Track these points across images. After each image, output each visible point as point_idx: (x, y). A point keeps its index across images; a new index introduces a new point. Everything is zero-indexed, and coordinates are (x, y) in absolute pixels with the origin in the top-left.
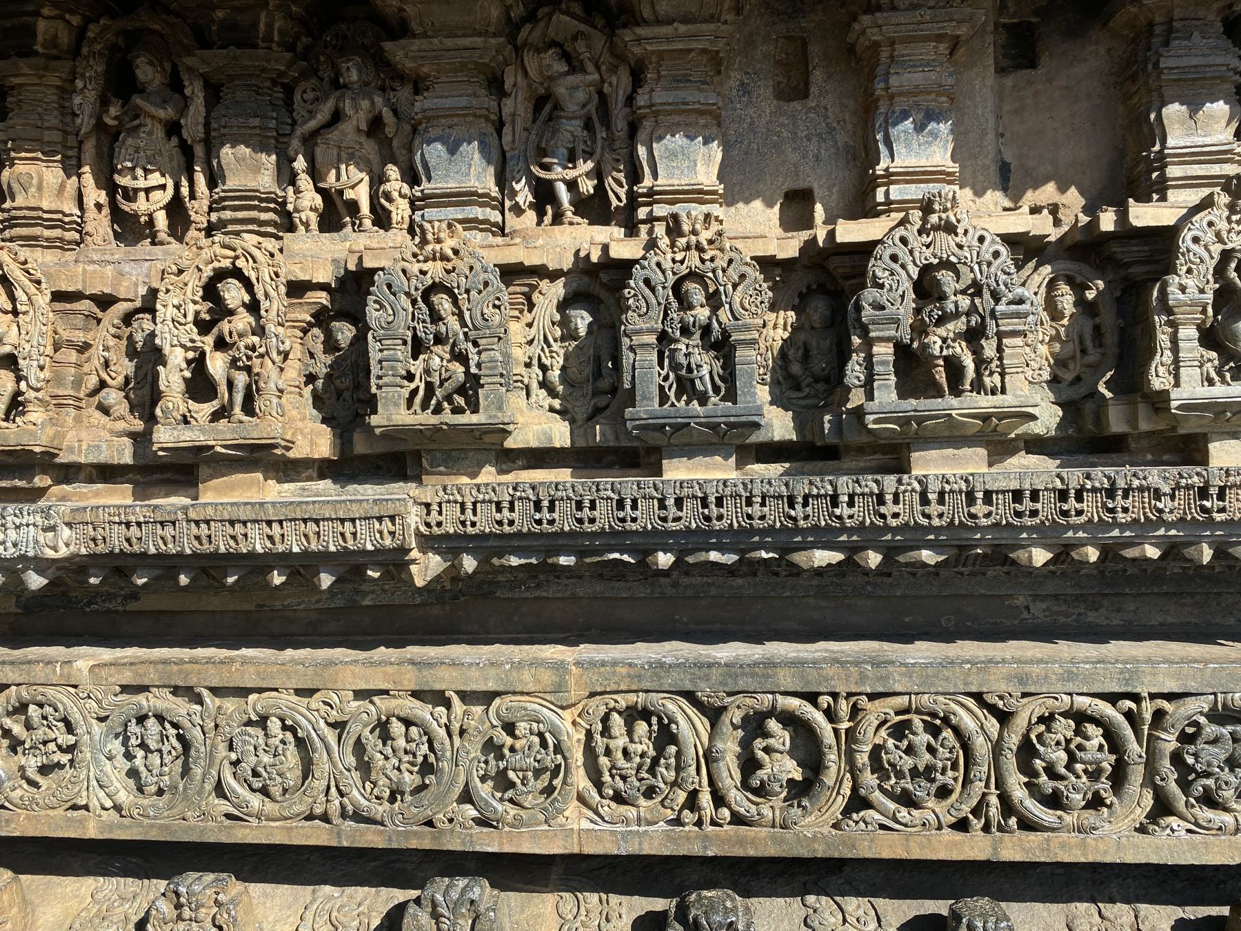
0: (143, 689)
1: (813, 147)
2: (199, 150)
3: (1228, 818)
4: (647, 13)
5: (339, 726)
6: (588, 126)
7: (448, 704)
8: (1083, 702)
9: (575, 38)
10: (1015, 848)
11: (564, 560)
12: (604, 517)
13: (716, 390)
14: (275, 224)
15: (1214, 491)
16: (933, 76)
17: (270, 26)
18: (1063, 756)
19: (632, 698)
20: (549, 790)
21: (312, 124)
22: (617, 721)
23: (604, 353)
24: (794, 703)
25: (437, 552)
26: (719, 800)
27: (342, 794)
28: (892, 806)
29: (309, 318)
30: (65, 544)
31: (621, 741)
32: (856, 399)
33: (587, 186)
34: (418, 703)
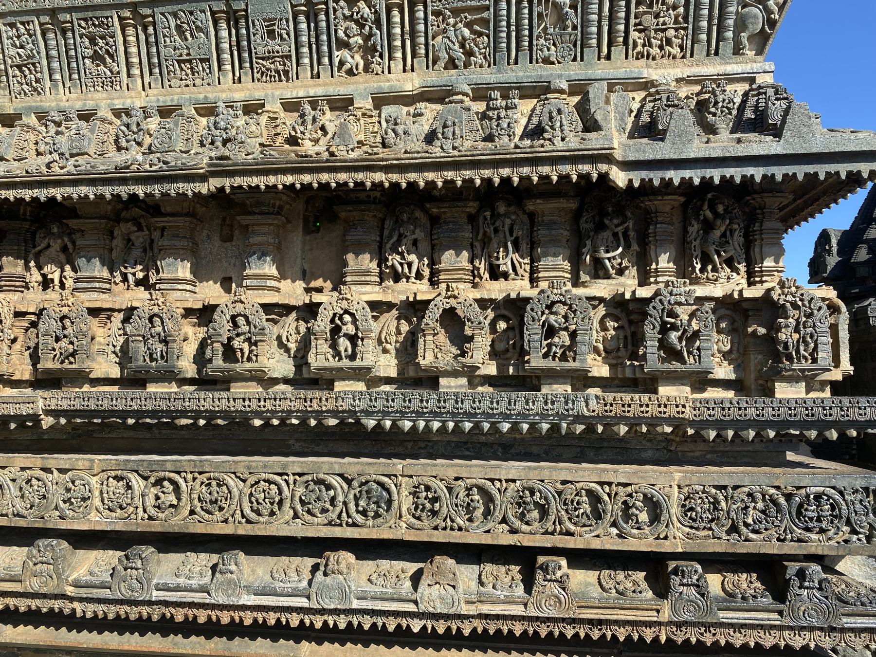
1: (233, 261)
3: (316, 519)
5: (14, 480)
6: (145, 251)
7: (52, 473)
8: (267, 476)
10: (244, 530)
11: (95, 421)
13: (162, 357)
14: (22, 287)
15: (308, 400)
16: (265, 239)
17: (25, 211)
18: (262, 495)
19: (116, 472)
21: (39, 248)
24: (172, 475)
25: (51, 416)
28: (203, 513)
29: (27, 325)
31: (112, 489)
34: (42, 472)
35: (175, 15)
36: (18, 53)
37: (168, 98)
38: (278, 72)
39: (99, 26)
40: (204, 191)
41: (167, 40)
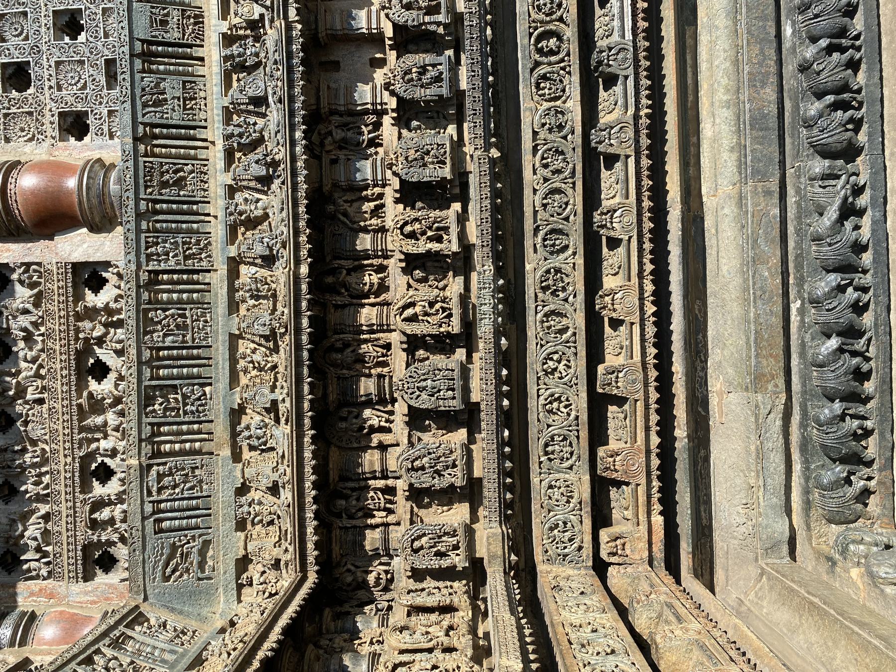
0: (535, 245)
2: (356, 263)
4: (314, 107)
5: (546, 180)
6: (348, 130)
7: (537, 145)
9: (319, 134)
12: (478, 94)
20: (562, 113)
22: (540, 92)
23: (425, 115)
24: (532, 39)
26: (562, 60)
27: (566, 178)
30: (489, 267)
31: (547, 91)
32: (441, 30)
33: (370, 127)
35: (145, 105)
36: (173, 257)
37: (216, 118)
38: (195, 24)
39: (152, 176)
40: (299, 27)
41: (165, 116)
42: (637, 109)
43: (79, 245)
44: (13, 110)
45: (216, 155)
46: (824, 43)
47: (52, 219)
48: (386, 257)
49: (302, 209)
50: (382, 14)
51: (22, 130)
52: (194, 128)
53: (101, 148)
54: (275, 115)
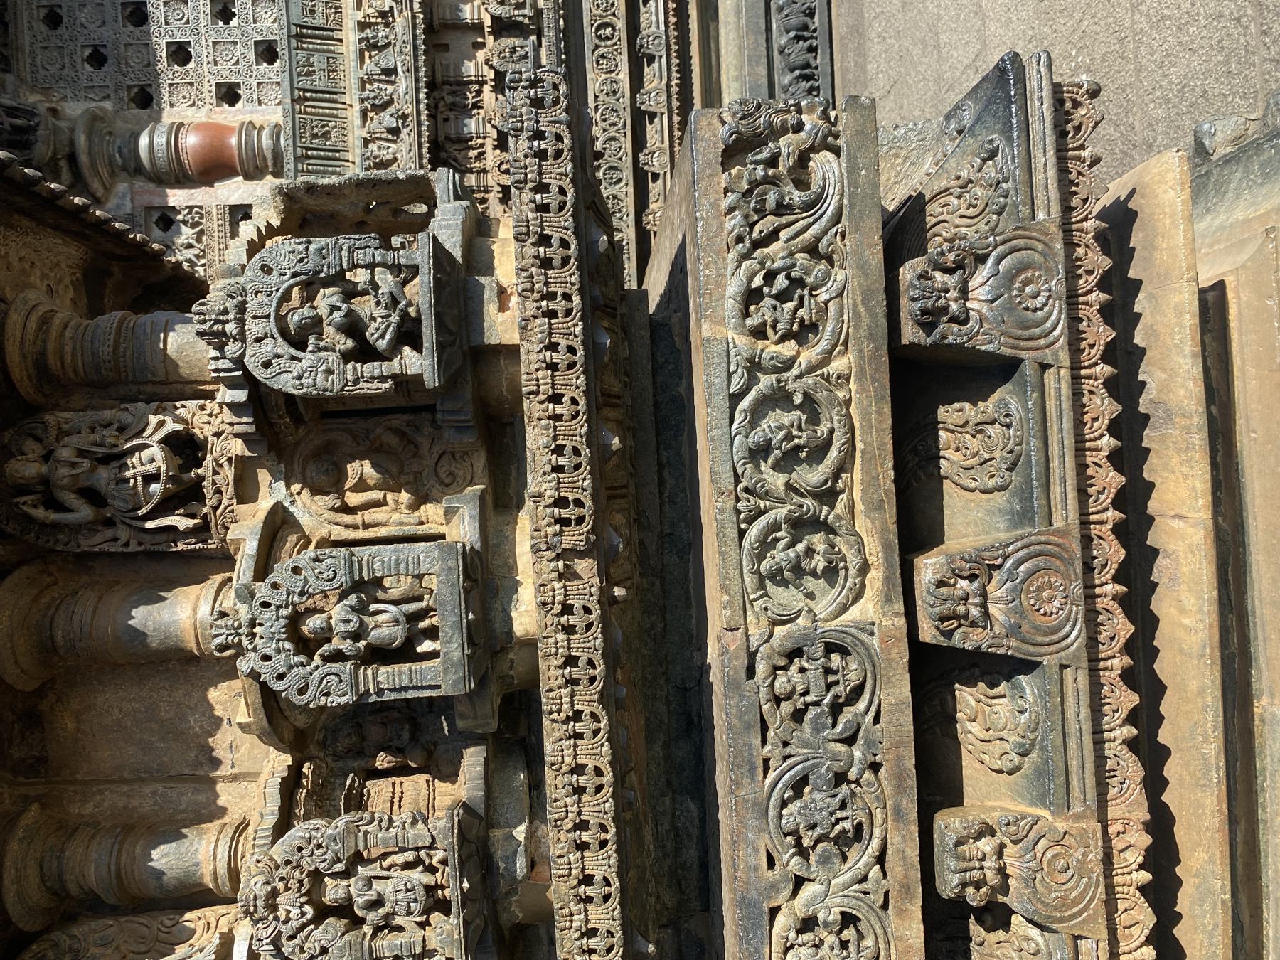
5: (605, 130)
32: (527, 21)
35: (299, 75)
42: (669, 79)
43: (233, 190)
44: (177, 81)
45: (354, 115)
46: (792, 34)
47: (213, 169)
48: (487, 192)
49: (425, 150)
50: (482, 8)
51: (184, 97)
52: (335, 93)
53: (252, 112)
54: (403, 83)
